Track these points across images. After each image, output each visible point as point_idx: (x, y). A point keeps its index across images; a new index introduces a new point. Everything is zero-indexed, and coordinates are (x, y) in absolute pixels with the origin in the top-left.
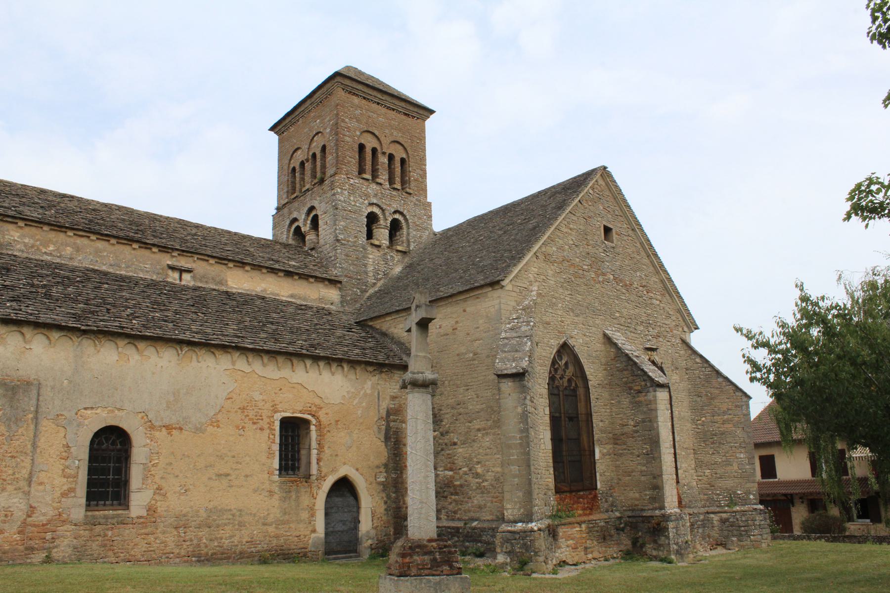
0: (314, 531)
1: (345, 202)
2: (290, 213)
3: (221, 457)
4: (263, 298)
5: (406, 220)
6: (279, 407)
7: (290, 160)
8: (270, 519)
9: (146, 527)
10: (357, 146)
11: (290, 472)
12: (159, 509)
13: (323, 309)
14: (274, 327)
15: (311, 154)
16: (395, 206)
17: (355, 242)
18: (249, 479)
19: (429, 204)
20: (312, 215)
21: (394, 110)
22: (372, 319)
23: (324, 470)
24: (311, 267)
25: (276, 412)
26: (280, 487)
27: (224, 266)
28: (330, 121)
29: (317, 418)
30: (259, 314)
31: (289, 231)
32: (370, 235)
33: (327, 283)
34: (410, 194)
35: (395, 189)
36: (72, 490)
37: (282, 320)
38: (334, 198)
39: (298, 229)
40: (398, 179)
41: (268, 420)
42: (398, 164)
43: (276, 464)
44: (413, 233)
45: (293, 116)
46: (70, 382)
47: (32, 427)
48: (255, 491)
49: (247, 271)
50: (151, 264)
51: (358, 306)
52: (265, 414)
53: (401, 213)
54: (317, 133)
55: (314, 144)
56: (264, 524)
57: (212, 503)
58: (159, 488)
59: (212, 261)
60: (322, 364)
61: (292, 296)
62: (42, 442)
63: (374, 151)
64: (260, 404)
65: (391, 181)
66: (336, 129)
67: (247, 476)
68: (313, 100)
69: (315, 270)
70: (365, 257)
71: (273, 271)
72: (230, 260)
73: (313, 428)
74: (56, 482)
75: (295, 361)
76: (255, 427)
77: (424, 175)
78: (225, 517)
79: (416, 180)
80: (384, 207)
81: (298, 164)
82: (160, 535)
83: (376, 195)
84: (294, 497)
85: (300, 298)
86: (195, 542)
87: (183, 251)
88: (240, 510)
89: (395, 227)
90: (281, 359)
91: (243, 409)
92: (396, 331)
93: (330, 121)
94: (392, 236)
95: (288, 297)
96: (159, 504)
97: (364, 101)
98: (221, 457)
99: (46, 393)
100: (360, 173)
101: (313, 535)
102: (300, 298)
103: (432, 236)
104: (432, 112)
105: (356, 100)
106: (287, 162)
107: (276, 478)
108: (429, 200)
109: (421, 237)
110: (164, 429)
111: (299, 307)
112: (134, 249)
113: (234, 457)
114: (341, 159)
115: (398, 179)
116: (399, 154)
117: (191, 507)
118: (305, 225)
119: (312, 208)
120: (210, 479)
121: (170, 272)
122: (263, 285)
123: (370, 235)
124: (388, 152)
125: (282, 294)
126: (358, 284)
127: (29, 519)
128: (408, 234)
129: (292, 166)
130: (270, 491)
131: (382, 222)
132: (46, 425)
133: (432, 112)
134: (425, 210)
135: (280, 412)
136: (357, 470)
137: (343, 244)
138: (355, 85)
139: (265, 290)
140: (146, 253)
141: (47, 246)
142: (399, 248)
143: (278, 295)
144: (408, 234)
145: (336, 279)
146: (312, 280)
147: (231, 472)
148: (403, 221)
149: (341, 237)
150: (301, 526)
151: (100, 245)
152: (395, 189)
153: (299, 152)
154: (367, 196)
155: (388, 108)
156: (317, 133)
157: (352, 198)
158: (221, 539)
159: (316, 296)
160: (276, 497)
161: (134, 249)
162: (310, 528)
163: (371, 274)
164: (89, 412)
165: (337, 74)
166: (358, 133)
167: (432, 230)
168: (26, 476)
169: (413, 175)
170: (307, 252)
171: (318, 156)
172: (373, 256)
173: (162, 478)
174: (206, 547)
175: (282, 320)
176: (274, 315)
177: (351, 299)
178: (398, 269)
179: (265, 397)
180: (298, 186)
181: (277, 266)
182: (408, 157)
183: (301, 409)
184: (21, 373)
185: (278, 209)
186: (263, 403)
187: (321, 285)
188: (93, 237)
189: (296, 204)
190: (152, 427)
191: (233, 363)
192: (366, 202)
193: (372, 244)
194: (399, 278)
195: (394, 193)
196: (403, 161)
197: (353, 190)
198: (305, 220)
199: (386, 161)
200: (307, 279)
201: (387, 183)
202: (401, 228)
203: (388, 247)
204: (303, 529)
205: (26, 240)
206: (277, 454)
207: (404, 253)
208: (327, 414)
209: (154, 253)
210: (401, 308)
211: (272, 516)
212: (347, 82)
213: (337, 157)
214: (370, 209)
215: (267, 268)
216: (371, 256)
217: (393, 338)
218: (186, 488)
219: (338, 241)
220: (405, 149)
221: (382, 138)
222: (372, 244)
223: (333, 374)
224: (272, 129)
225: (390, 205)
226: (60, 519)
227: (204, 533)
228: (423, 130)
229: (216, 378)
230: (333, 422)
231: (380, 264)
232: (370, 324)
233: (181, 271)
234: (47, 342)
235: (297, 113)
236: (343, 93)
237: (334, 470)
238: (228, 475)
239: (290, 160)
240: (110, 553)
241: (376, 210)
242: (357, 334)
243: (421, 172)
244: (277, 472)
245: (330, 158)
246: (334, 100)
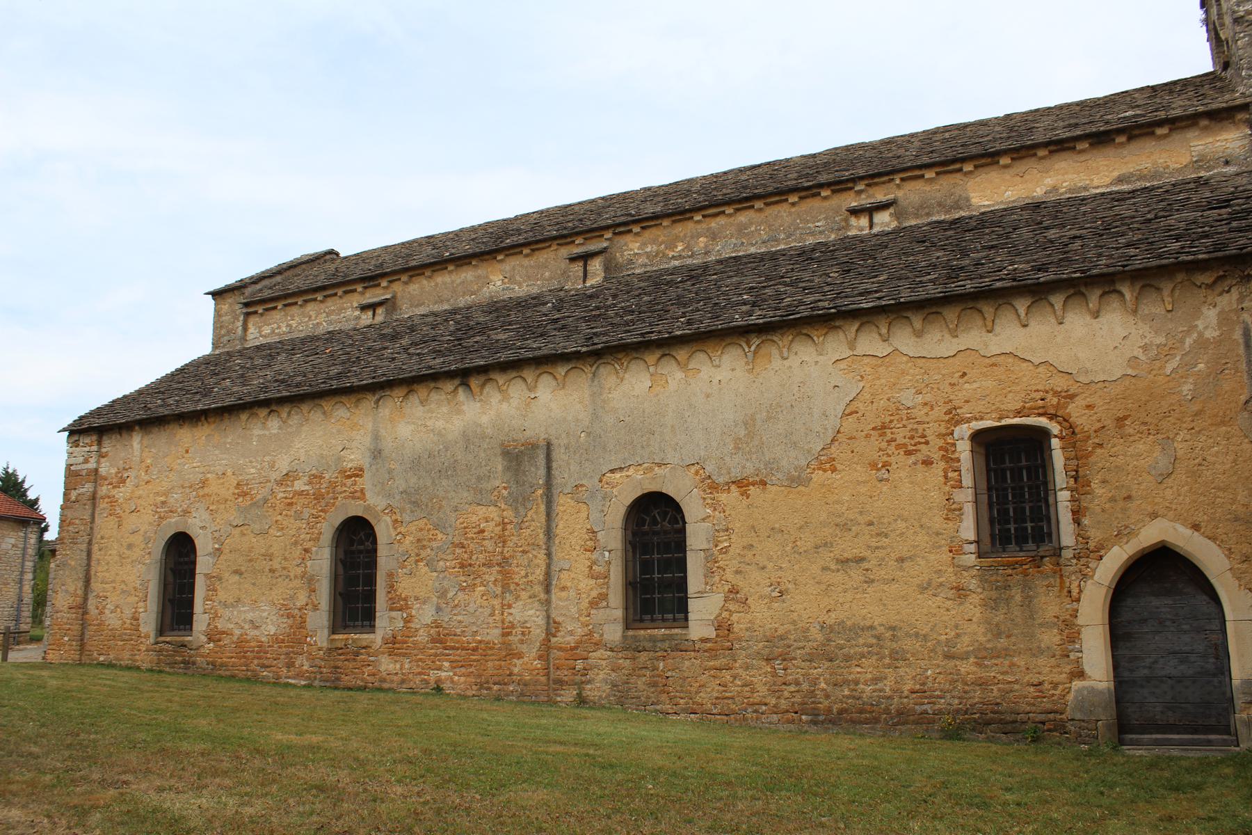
0: (1081, 674)
3: (845, 527)
6: (965, 411)
8: (964, 645)
9: (716, 657)
11: (1013, 547)
12: (736, 628)
18: (906, 564)
23: (1095, 535)
25: (957, 423)
26: (982, 580)
27: (958, 175)
29: (1065, 421)
33: (1204, 122)
36: (604, 597)
41: (941, 443)
43: (968, 530)
46: (589, 434)
47: (543, 508)
48: (923, 589)
49: (1006, 167)
50: (826, 219)
52: (932, 431)
56: (948, 657)
57: (833, 615)
58: (734, 590)
59: (929, 174)
60: (1057, 300)
61: (1120, 180)
62: (560, 528)
64: (920, 413)
67: (901, 560)
72: (963, 160)
73: (1055, 443)
74: (582, 585)
75: (988, 310)
76: (913, 459)
78: (861, 641)
82: (740, 671)
84: (1018, 598)
86: (805, 686)
87: (873, 176)
88: (893, 628)
90: (951, 314)
91: (882, 428)
96: (735, 617)
98: (845, 527)
99: (559, 455)
101: (1077, 684)
107: (971, 559)
110: (733, 487)
112: (793, 204)
113: (871, 524)
117: (794, 623)
120: (825, 569)
121: (853, 221)
122: (1049, 181)
125: (1096, 183)
127: (553, 640)
130: (958, 589)
132: (564, 504)
135: (968, 421)
136: (1196, 527)
139: (1055, 189)
140: (814, 203)
141: (672, 246)
147: (867, 554)
150: (1041, 661)
151: (743, 218)
158: (857, 683)
160: (975, 599)
161: (793, 204)
162: (1067, 669)
164: (618, 475)
168: (541, 578)
173: (737, 572)
174: (827, 697)
179: (928, 398)
183: (1018, 406)
184: (528, 433)
186: (927, 409)
187: (1191, 134)
188: (729, 210)
190: (714, 487)
191: (852, 346)
204: (1048, 670)
205: (648, 249)
206: (969, 509)
208: (1089, 407)
209: (826, 198)
211: (966, 640)
215: (1045, 145)
218: (783, 587)
223: (1096, 315)
226: (591, 642)
227: (820, 670)
229: (816, 378)
230: (1109, 423)
233: (871, 211)
234: (554, 383)
237: (1122, 535)
238: (862, 559)
240: (664, 697)
244: (973, 548)
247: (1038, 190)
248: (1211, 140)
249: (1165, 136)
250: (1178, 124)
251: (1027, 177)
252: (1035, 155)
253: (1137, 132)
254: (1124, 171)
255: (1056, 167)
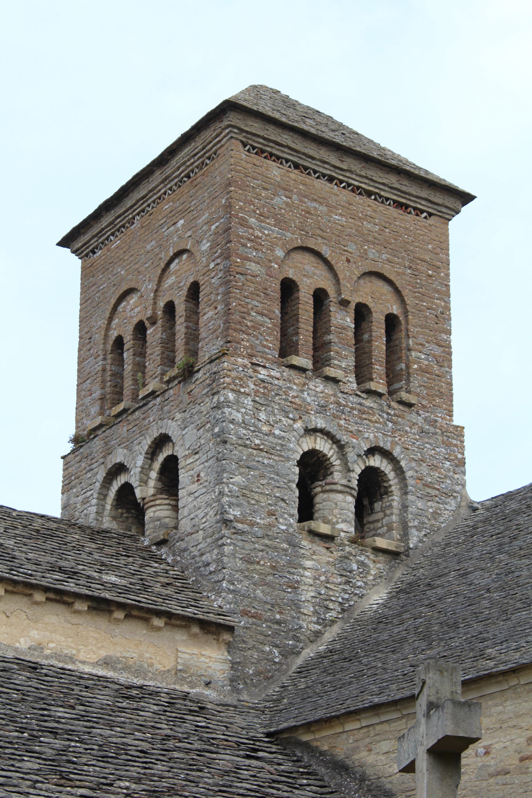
1: (245, 424)
2: (109, 452)
4: (34, 667)
5: (399, 471)
7: (111, 319)
10: (277, 286)
13: (186, 696)
14: (58, 743)
15: (161, 304)
16: (372, 436)
17: (270, 526)
19: (459, 431)
20: (161, 458)
21: (369, 194)
22: (309, 726)
24: (158, 588)
28: (209, 222)
30: (21, 707)
31: (103, 496)
32: (306, 510)
33: (196, 629)
34: (410, 405)
35: (370, 393)
37: (79, 726)
38: (218, 414)
39: (127, 490)
40: (379, 368)
42: (378, 330)
44: (416, 504)
45: (119, 210)
51: (274, 689)
53: (386, 454)
54: (178, 254)
55: (170, 281)
61: (107, 663)
63: (320, 296)
65: (362, 372)
66: (225, 243)
68: (168, 170)
69: (168, 597)
70: (295, 564)
71: (60, 597)
77: (445, 358)
79: (424, 371)
80: (344, 438)
81: (130, 328)
83: (323, 409)
85: (126, 668)
89: (370, 489)
92: (370, 759)
93: (209, 222)
94: (362, 511)
95: (96, 664)
97: (295, 174)
100: (283, 354)
102: (126, 668)
103: (464, 512)
104: (466, 198)
105: (275, 171)
106: (102, 323)
108: (457, 421)
109: (436, 515)
111: (125, 692)
114: (236, 317)
115: (379, 368)
116: (382, 304)
118: (144, 482)
119: (163, 440)
122: (36, 635)
123: (306, 510)
124: (355, 300)
125: (82, 656)
126: (276, 633)
128: (405, 507)
129: (114, 334)
131: (337, 476)
133: (466, 198)
134: (448, 445)
137: (239, 532)
138: (272, 133)
139: (39, 647)
142: (381, 543)
143: (72, 659)
144: (405, 507)
145: (220, 620)
146: (158, 622)
148: (391, 475)
149: (234, 513)
152: (370, 393)
153: (133, 299)
154: (302, 410)
155: (356, 190)
156: (178, 254)
157: (262, 416)
159: (169, 664)
163: (308, 609)
165: (228, 107)
166: (280, 253)
167: (464, 497)
169: (418, 357)
170: (146, 549)
171: (181, 309)
172: (315, 560)
175: (79, 726)
176: (60, 712)
177: (257, 673)
178: (377, 597)
180: (128, 383)
181: (71, 586)
182: (406, 312)
185: (78, 441)
187: (180, 636)
189: (122, 429)
192: (298, 425)
193: (313, 533)
194: (380, 620)
195: (369, 403)
196: (391, 322)
197: (266, 395)
198: (145, 471)
199: (349, 321)
200: (147, 620)
201: (352, 378)
202: (387, 492)
203: (353, 541)
207: (393, 555)
210: (383, 699)
212: (255, 126)
213: (228, 312)
214: (308, 444)
216: (308, 564)
217: (363, 779)
219: (226, 522)
220: (397, 291)
221: (340, 266)
222: (313, 533)
224: (66, 242)
225: (358, 434)
228: (443, 245)
231: (331, 584)
232: (306, 738)
235: (129, 202)
236: (241, 153)
239: (111, 319)
241: (322, 445)
242: (270, 765)
243: (438, 351)
245: (208, 315)
246: (219, 171)
247: (22, 640)
248: (196, 651)
249: (159, 629)
250: (174, 621)
251: (13, 619)
252: (30, 595)
253: (135, 613)
254: (111, 653)
255: (46, 619)
